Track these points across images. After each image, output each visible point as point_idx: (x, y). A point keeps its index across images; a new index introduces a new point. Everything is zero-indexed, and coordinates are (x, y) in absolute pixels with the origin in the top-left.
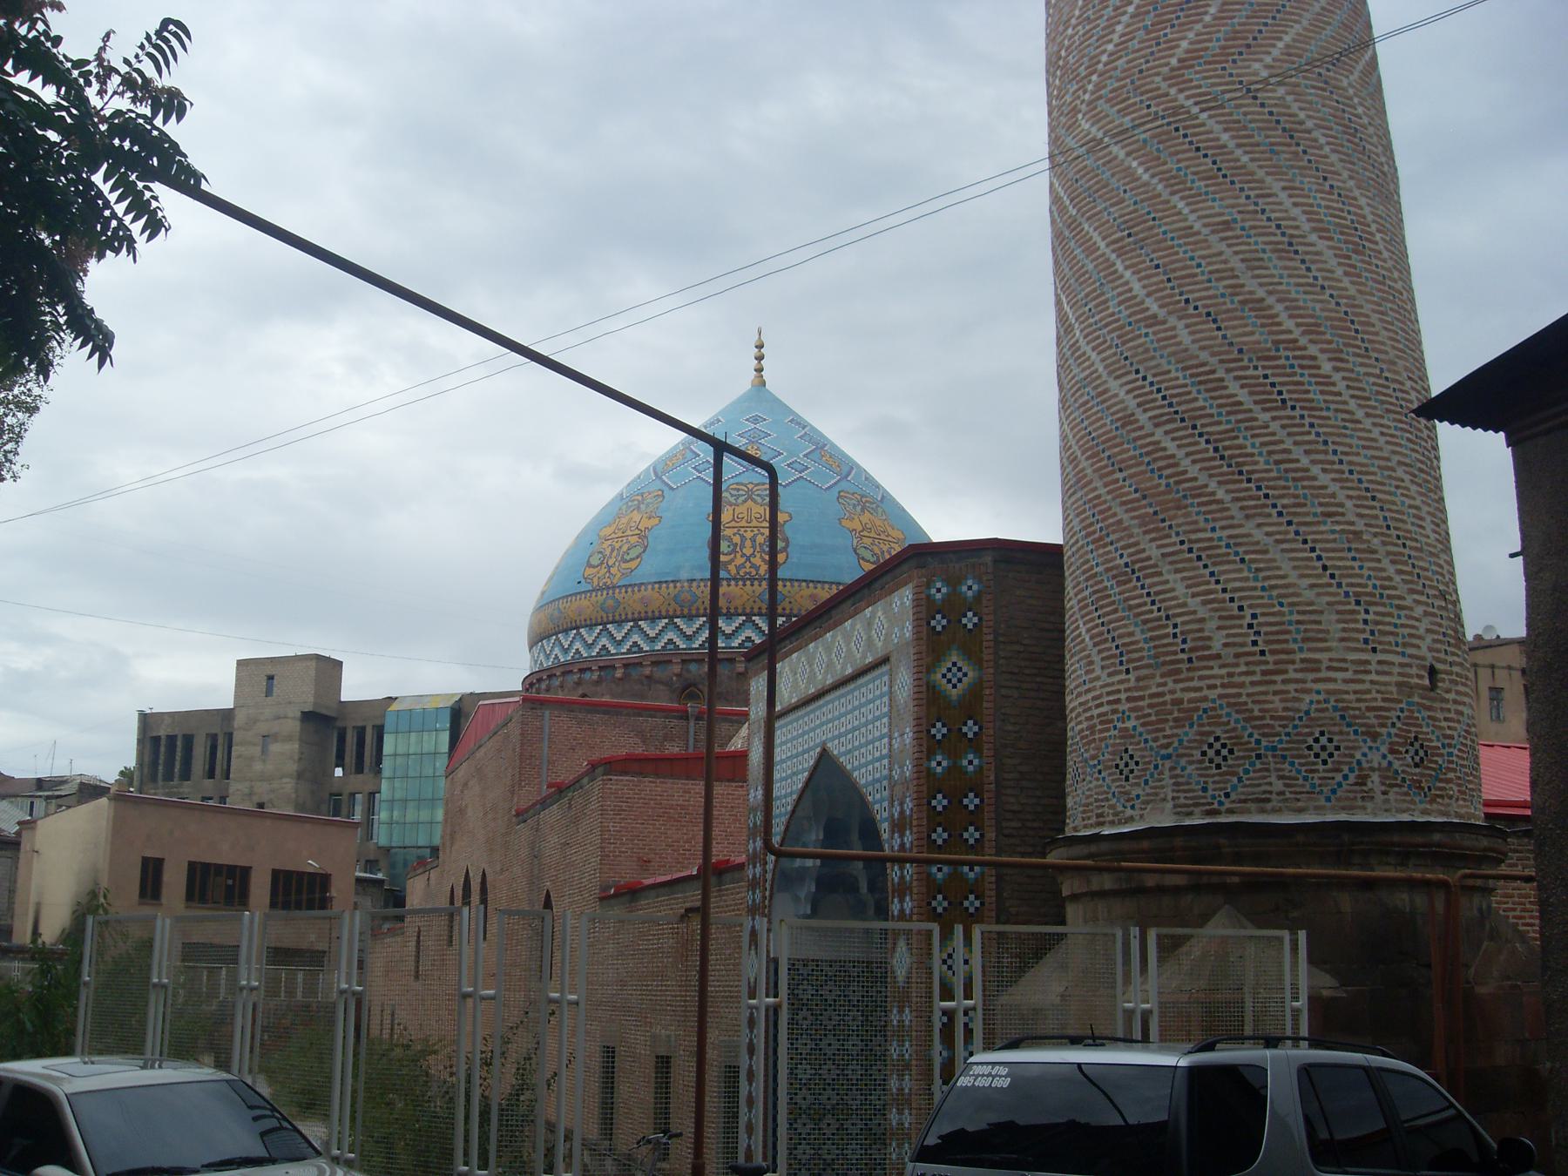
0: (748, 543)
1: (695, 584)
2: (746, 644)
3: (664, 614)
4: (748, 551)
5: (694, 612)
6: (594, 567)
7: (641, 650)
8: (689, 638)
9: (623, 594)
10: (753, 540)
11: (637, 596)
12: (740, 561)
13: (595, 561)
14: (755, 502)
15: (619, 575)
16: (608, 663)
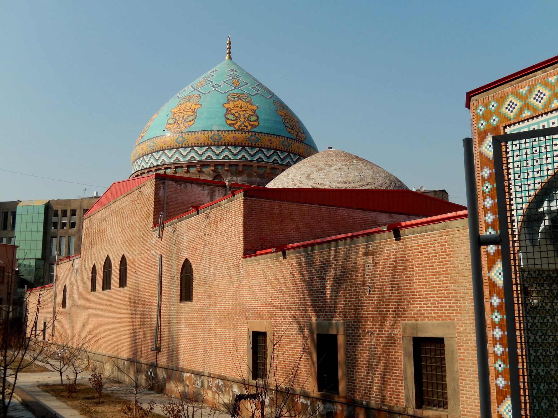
0: (242, 117)
1: (220, 132)
2: (243, 159)
3: (206, 144)
4: (242, 120)
5: (220, 144)
6: (171, 124)
7: (195, 159)
8: (218, 155)
9: (187, 135)
10: (244, 115)
11: (194, 136)
12: (239, 123)
13: (171, 121)
14: (241, 100)
15: (184, 127)
16: (180, 165)
